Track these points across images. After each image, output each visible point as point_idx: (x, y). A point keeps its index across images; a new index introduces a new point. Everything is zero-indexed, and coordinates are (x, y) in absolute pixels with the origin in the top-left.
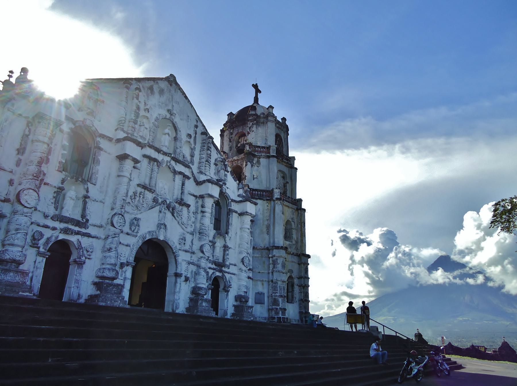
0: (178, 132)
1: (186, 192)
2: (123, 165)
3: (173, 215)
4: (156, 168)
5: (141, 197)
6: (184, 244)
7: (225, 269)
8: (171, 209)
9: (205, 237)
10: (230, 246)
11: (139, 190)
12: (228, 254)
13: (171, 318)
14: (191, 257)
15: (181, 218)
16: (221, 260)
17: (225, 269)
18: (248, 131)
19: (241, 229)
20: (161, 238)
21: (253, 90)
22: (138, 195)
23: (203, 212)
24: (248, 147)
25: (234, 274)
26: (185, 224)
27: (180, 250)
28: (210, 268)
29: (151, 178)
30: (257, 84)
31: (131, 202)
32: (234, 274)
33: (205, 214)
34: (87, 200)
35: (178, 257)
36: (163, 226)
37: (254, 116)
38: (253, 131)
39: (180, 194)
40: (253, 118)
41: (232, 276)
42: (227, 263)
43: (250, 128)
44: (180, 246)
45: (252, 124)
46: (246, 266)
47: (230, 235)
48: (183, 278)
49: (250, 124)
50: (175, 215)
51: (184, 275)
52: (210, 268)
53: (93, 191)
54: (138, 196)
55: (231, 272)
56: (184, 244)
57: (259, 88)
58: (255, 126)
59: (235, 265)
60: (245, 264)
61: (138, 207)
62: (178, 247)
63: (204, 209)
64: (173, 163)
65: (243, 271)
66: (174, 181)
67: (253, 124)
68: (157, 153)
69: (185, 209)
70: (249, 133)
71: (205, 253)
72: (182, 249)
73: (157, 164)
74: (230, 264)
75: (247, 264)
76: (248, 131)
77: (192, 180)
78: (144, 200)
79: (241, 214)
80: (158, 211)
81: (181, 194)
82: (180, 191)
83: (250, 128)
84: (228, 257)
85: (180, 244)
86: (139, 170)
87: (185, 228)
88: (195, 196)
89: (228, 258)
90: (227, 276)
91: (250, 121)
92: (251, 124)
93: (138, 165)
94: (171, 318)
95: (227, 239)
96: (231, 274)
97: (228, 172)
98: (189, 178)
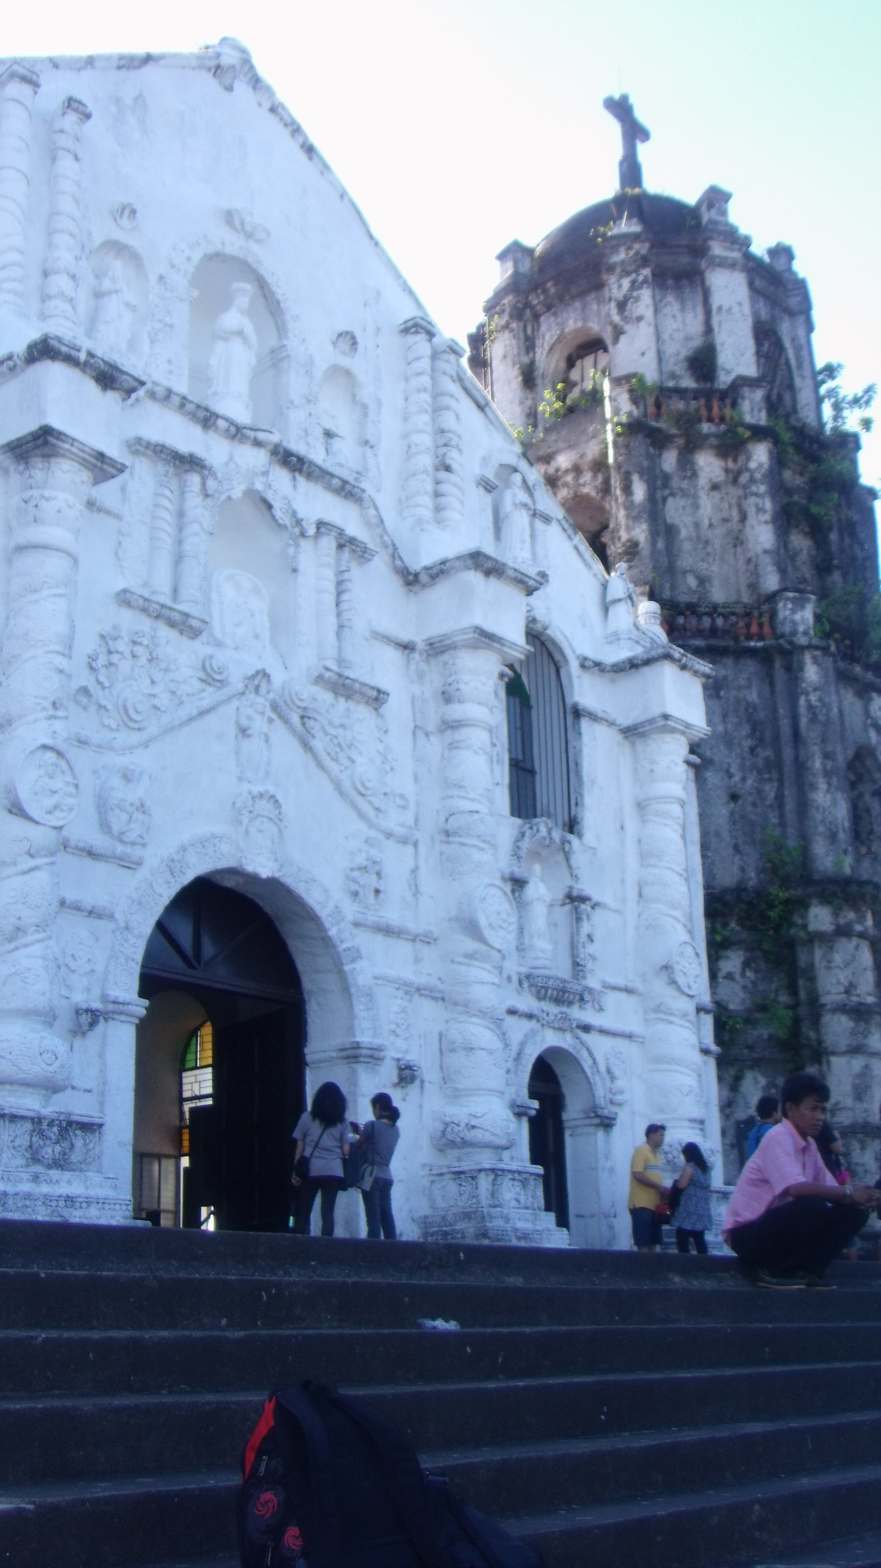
0: (291, 325)
1: (360, 625)
2: (35, 493)
3: (307, 746)
4: (194, 502)
5: (143, 660)
6: (377, 891)
7: (588, 1016)
8: (295, 719)
9: (476, 855)
11: (128, 620)
12: (590, 938)
13: (452, 1326)
14: (417, 960)
15: (346, 762)
16: (562, 970)
18: (616, 318)
19: (641, 806)
21: (614, 128)
26: (369, 793)
27: (356, 924)
28: (512, 1012)
29: (179, 559)
30: (624, 99)
31: (92, 686)
32: (629, 1036)
33: (463, 734)
35: (353, 961)
36: (264, 806)
38: (640, 319)
39: (332, 638)
40: (632, 253)
41: (621, 1044)
42: (593, 982)
43: (622, 306)
44: (356, 907)
45: (633, 282)
46: (686, 990)
49: (620, 286)
50: (318, 744)
52: (512, 1012)
54: (127, 653)
56: (377, 891)
57: (641, 115)
58: (646, 295)
59: (628, 991)
60: (681, 980)
61: (132, 713)
62: (350, 910)
63: (456, 711)
64: (281, 477)
65: (672, 1018)
66: (295, 570)
67: (634, 286)
68: (196, 430)
69: (362, 712)
70: (618, 333)
71: (487, 933)
72: (371, 918)
73: (204, 484)
74: (608, 987)
75: (692, 983)
76: (616, 318)
77: (380, 564)
78: (158, 676)
80: (232, 730)
81: (338, 635)
82: (331, 622)
83: (622, 306)
84: (591, 949)
85: (356, 894)
86: (118, 517)
87: (371, 813)
88: (407, 647)
89: (593, 958)
91: (618, 270)
92: (626, 283)
93: (107, 492)
94: (452, 1326)
95: (579, 859)
97: (547, 519)
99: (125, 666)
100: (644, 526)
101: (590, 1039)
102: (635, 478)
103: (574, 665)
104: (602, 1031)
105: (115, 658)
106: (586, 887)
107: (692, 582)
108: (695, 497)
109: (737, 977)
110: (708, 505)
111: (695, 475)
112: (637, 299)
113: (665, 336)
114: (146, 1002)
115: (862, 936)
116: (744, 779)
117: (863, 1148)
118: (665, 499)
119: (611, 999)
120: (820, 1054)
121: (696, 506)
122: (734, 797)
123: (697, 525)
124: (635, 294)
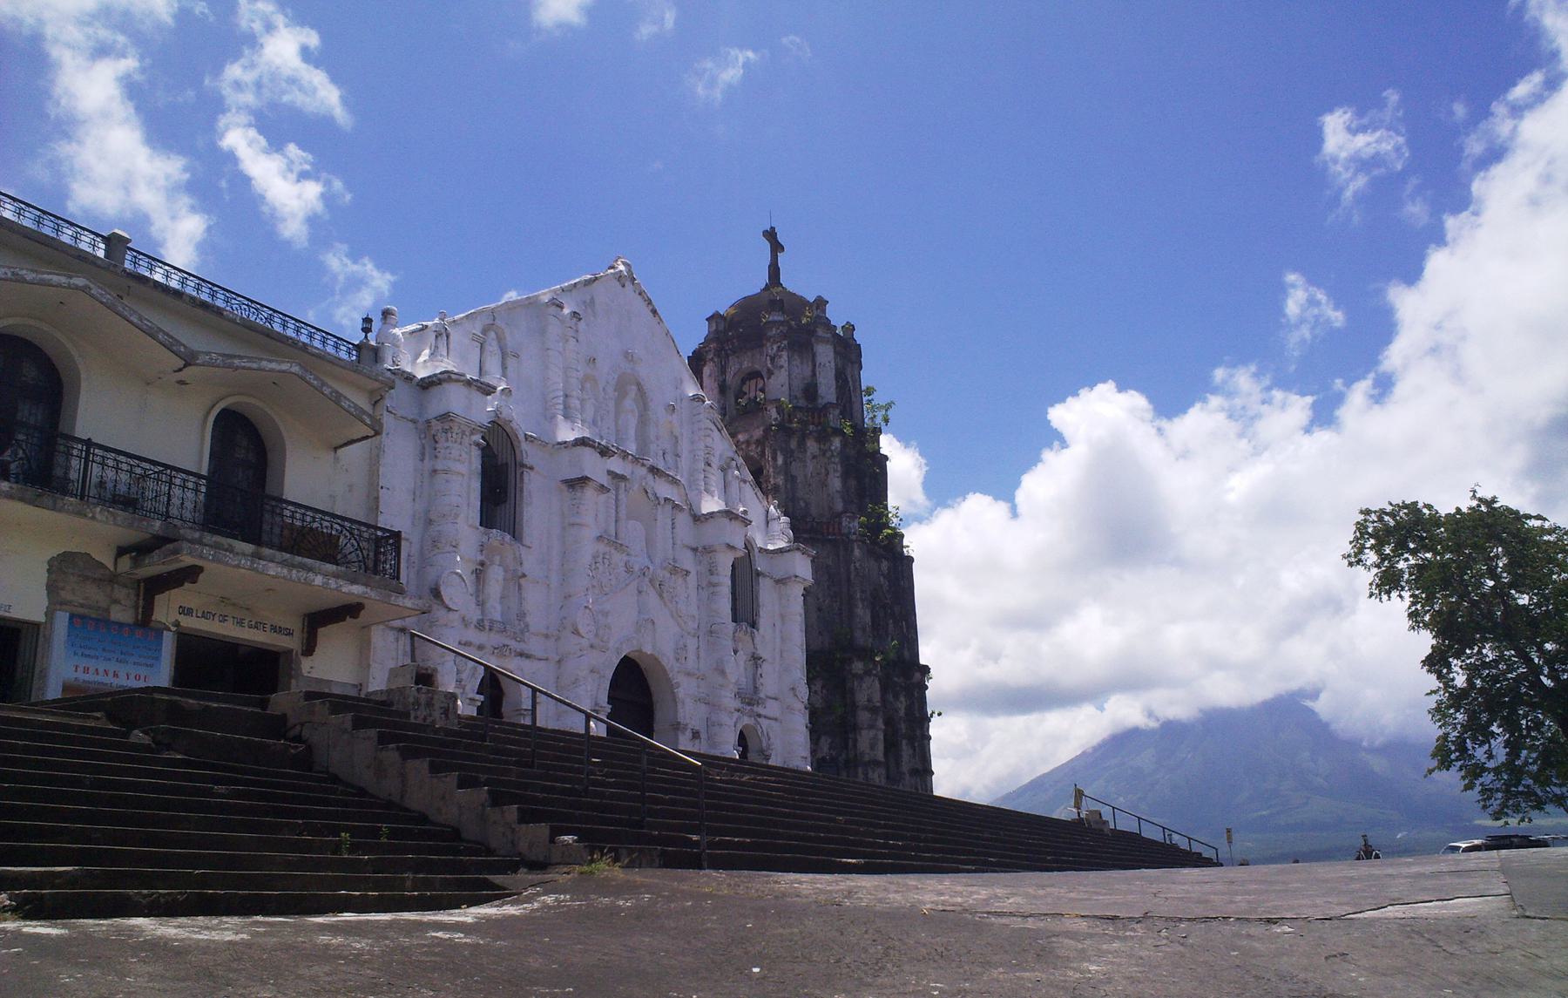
3: (661, 596)
7: (760, 710)
10: (764, 656)
11: (602, 547)
14: (698, 687)
17: (760, 710)
20: (648, 650)
22: (600, 560)
23: (712, 585)
24: (775, 410)
25: (776, 719)
32: (776, 719)
33: (718, 589)
34: (523, 581)
35: (677, 688)
37: (781, 328)
38: (782, 367)
41: (772, 722)
42: (762, 695)
44: (678, 665)
47: (761, 630)
48: (689, 734)
51: (690, 726)
53: (530, 563)
55: (771, 715)
58: (785, 354)
59: (776, 699)
74: (767, 697)
79: (780, 582)
84: (761, 680)
90: (764, 722)
95: (758, 639)
96: (770, 719)
97: (745, 482)
98: (682, 509)
99: (601, 568)
100: (782, 477)
101: (764, 722)
102: (779, 453)
103: (756, 550)
104: (765, 717)
105: (598, 565)
106: (761, 652)
107: (802, 504)
108: (805, 461)
109: (820, 693)
110: (811, 466)
111: (805, 451)
112: (780, 357)
113: (793, 376)
114: (610, 706)
115: (875, 675)
116: (824, 601)
117: (873, 772)
118: (791, 463)
119: (770, 703)
120: (855, 728)
121: (805, 466)
122: (820, 610)
123: (805, 476)
124: (779, 354)
